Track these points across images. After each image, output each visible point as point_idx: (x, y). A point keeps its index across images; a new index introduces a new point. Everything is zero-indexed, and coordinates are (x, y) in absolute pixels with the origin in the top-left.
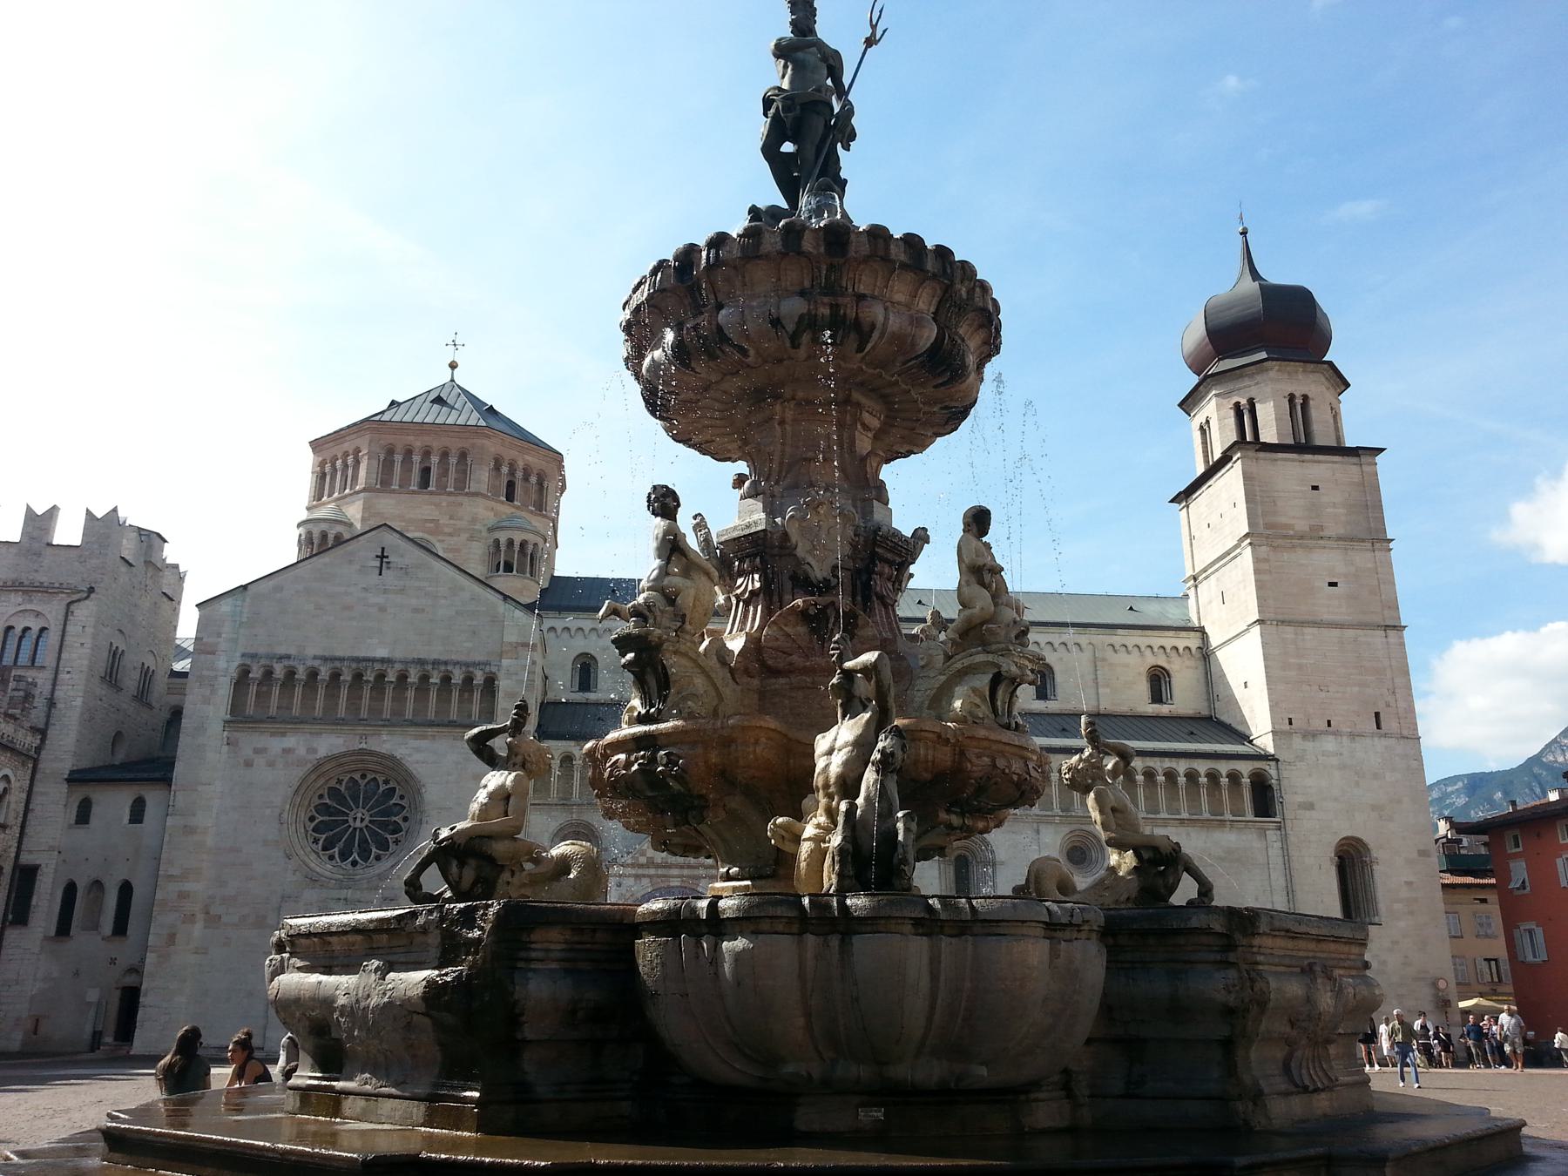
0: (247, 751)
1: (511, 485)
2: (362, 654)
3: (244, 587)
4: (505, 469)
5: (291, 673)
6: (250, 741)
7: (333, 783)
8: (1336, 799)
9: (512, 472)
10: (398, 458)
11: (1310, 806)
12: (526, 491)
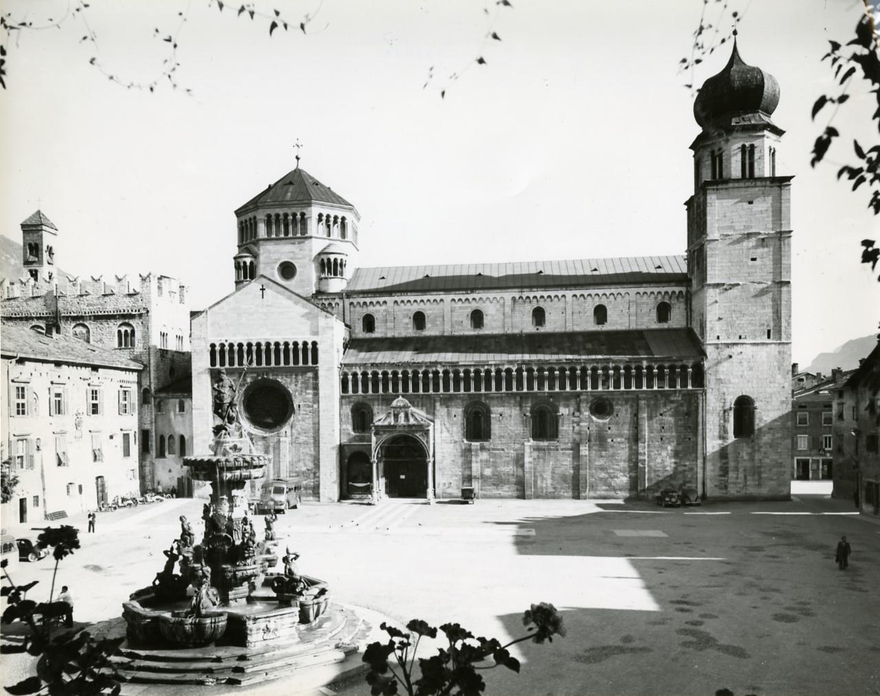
1: (328, 226)
9: (328, 221)
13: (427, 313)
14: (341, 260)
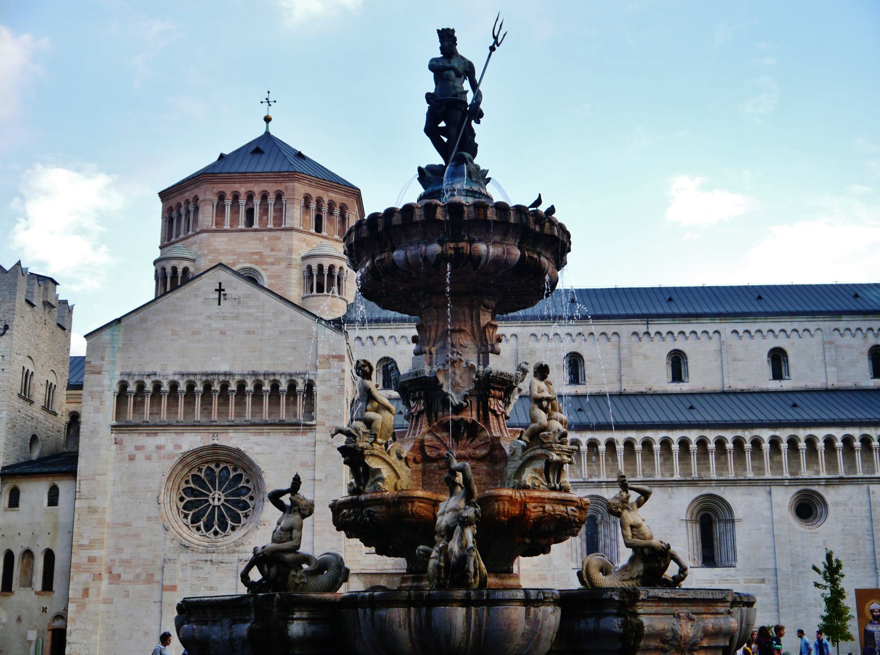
0: (130, 449)
1: (319, 219)
2: (209, 369)
3: (118, 321)
4: (313, 205)
5: (157, 386)
6: (132, 440)
7: (195, 472)
9: (319, 209)
10: (228, 202)
12: (331, 222)
14: (341, 268)
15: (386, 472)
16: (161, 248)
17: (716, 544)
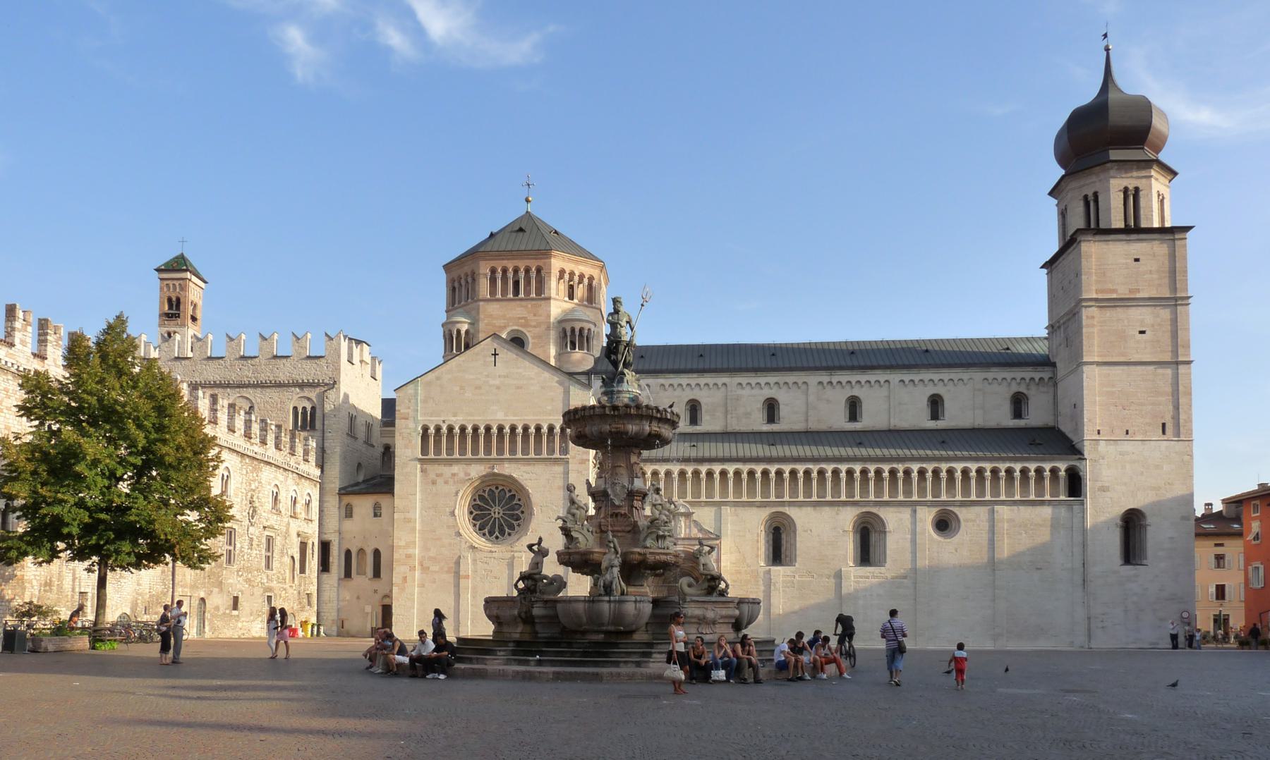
4: (567, 277)
6: (434, 469)
8: (1125, 484)
9: (571, 279)
10: (499, 275)
11: (1104, 489)
13: (703, 401)
15: (581, 538)
16: (447, 312)
17: (872, 550)
